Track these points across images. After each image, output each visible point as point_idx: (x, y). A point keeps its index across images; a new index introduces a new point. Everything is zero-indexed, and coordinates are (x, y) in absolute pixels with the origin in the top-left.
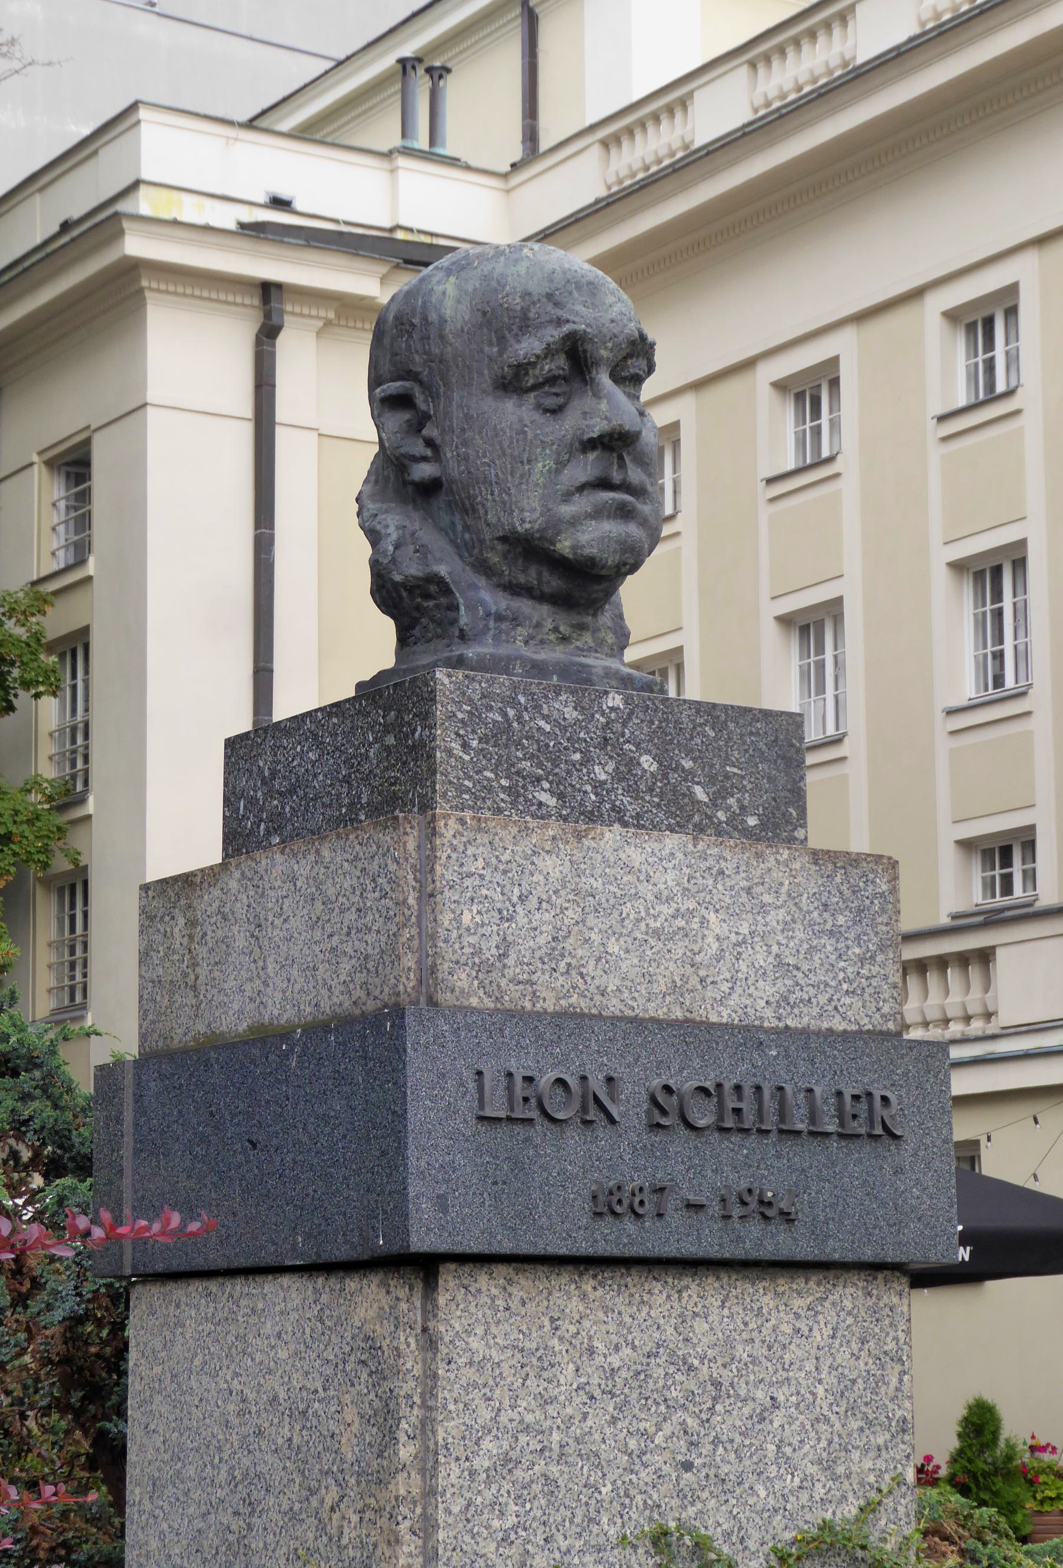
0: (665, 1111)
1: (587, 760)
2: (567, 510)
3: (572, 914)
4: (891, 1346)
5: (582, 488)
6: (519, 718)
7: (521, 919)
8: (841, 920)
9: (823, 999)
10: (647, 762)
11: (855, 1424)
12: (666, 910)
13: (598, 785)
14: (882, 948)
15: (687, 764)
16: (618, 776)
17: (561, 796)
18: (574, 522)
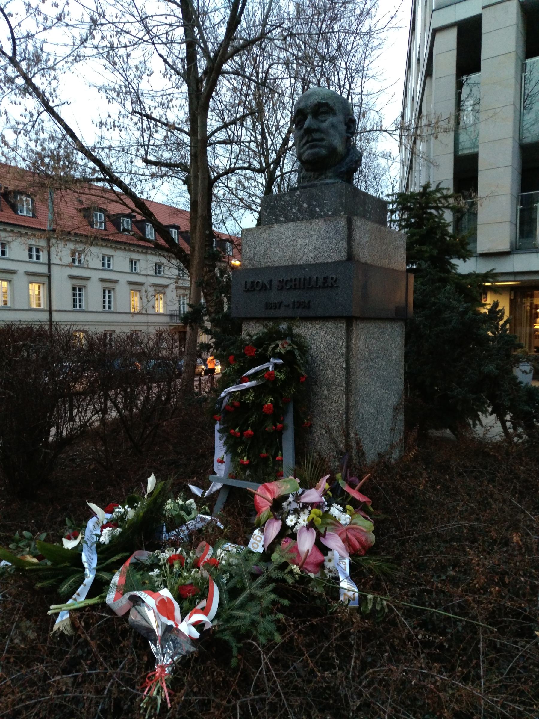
0: (283, 285)
1: (292, 208)
2: (302, 151)
3: (268, 245)
4: (340, 336)
5: (305, 144)
6: (277, 203)
7: (258, 248)
8: (331, 234)
9: (326, 255)
10: (305, 205)
11: (330, 353)
12: (288, 240)
13: (294, 213)
14: (342, 239)
15: (314, 203)
16: (298, 210)
17: (286, 218)
18: (304, 152)
